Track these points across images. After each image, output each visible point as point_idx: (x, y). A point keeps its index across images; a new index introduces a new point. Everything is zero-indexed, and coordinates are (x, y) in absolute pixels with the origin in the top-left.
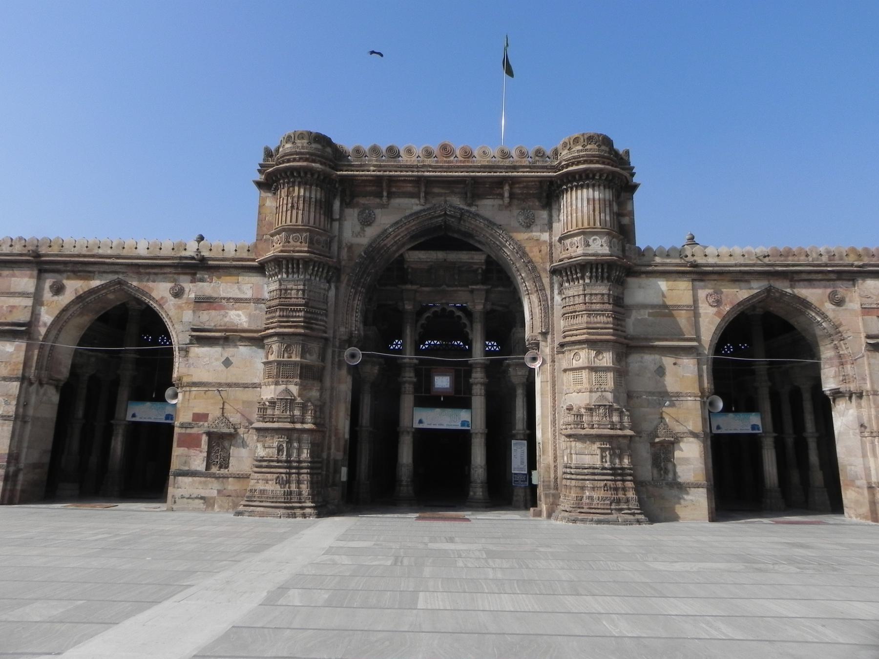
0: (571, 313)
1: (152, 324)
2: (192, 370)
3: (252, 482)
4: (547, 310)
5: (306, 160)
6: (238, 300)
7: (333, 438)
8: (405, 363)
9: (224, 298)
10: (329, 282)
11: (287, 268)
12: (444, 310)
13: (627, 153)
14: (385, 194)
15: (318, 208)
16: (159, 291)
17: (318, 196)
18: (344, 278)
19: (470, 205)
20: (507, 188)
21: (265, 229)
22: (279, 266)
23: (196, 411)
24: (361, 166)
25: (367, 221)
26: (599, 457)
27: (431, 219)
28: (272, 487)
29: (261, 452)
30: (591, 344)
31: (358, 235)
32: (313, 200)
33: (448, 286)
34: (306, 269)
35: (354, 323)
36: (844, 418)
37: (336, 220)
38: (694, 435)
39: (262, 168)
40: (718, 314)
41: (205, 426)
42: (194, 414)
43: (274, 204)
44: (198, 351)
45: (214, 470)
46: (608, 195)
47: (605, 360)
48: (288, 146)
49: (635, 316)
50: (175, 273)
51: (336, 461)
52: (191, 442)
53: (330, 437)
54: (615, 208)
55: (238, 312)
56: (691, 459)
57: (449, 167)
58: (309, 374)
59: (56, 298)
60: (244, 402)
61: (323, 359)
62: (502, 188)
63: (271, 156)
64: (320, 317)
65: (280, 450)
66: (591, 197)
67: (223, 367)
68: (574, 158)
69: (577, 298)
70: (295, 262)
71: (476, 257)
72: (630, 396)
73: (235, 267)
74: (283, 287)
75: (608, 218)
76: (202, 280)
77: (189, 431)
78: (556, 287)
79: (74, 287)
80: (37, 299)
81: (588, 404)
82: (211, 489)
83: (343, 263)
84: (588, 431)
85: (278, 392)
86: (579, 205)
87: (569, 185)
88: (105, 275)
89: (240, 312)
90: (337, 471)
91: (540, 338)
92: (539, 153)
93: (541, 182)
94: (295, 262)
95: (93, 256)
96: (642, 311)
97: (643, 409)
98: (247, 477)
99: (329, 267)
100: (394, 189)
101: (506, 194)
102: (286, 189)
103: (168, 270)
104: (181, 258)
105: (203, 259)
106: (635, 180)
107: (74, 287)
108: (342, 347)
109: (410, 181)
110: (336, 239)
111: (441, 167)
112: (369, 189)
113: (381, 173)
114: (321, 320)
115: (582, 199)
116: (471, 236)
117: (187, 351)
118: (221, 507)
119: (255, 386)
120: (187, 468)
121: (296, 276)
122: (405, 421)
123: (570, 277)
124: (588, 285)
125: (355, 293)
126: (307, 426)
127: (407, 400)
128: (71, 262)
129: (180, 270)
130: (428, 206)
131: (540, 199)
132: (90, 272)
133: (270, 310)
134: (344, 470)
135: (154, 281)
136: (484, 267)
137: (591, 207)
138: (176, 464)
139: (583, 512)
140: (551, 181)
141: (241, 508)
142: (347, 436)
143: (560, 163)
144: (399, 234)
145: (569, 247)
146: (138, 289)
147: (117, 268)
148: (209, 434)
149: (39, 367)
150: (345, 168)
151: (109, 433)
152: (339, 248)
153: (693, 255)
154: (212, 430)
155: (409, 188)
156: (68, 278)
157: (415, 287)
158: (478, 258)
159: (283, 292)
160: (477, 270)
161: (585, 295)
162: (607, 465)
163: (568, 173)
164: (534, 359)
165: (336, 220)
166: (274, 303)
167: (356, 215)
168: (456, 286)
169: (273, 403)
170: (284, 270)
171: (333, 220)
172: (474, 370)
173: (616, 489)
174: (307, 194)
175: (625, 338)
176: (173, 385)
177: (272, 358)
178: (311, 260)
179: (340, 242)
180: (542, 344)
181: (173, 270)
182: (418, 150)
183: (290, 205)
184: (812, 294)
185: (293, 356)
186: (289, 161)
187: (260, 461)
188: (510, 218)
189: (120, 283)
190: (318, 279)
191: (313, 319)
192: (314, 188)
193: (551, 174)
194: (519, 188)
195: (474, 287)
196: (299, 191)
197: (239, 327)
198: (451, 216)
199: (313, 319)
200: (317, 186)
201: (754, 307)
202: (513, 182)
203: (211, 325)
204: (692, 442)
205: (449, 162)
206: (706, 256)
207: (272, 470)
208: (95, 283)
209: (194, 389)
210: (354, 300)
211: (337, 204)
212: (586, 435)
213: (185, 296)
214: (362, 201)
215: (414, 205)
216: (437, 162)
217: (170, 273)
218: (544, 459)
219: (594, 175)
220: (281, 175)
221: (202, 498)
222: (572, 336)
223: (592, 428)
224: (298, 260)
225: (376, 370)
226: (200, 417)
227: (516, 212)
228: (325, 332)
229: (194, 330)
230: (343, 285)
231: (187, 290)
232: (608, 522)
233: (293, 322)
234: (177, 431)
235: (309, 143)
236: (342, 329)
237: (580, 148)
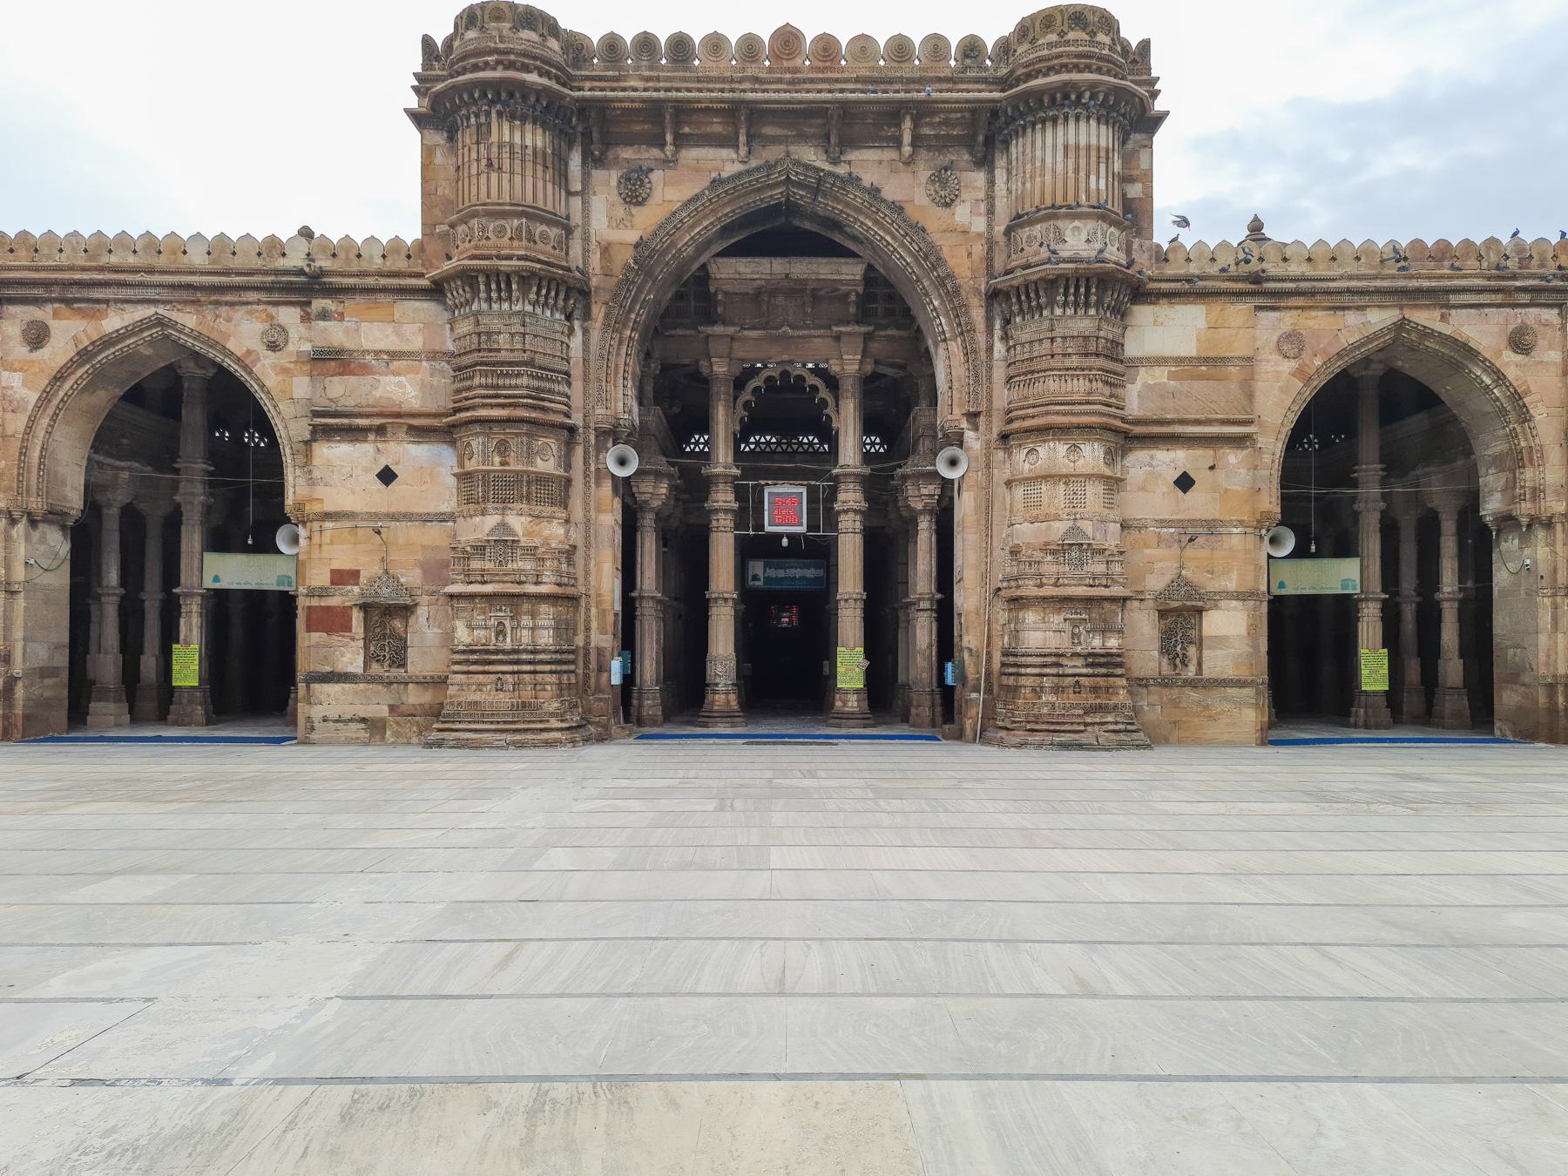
0: (1025, 374)
1: (233, 402)
2: (320, 491)
3: (452, 690)
5: (510, 66)
6: (394, 355)
7: (593, 610)
8: (717, 476)
9: (369, 352)
10: (569, 317)
11: (489, 290)
12: (785, 374)
13: (1145, 46)
14: (669, 138)
15: (540, 168)
16: (240, 335)
17: (539, 144)
18: (598, 312)
19: (835, 162)
20: (907, 124)
21: (437, 212)
22: (471, 286)
23: (336, 565)
24: (617, 79)
26: (1066, 636)
27: (759, 190)
29: (463, 635)
31: (620, 224)
32: (529, 151)
33: (792, 327)
34: (525, 295)
37: (577, 193)
38: (1241, 596)
39: (423, 84)
40: (1299, 372)
42: (333, 571)
43: (452, 161)
44: (332, 453)
45: (376, 668)
47: (1082, 461)
48: (471, 34)
49: (1144, 377)
50: (269, 303)
51: (600, 651)
52: (333, 621)
53: (588, 610)
54: (1117, 166)
55: (398, 379)
56: (1233, 635)
57: (792, 82)
59: (37, 355)
60: (424, 547)
61: (568, 467)
62: (899, 126)
63: (437, 58)
64: (556, 387)
65: (500, 632)
66: (1072, 141)
67: (379, 485)
68: (1041, 60)
69: (1036, 346)
70: (503, 279)
71: (844, 269)
73: (384, 290)
74: (482, 328)
75: (1102, 186)
76: (324, 315)
77: (325, 602)
78: (998, 325)
79: (69, 333)
81: (1047, 544)
83: (594, 282)
84: (1048, 591)
85: (487, 528)
86: (1049, 160)
87: (1030, 118)
88: (128, 307)
89: (402, 379)
90: (603, 668)
91: (964, 424)
92: (972, 47)
93: (973, 111)
94: (503, 279)
95: (101, 269)
96: (1157, 371)
97: (1147, 551)
98: (441, 682)
99: (569, 290)
100: (687, 130)
101: (907, 138)
102: (474, 129)
103: (252, 296)
104: (277, 272)
105: (323, 273)
106: (1159, 105)
107: (69, 333)
108: (600, 448)
109: (718, 112)
110: (578, 233)
111: (780, 81)
112: (637, 128)
113: (662, 94)
114: (559, 394)
115: (1055, 147)
116: (836, 225)
117: (308, 456)
118: (396, 734)
119: (443, 518)
120: (328, 669)
121: (506, 306)
123: (1025, 306)
124: (1060, 318)
125: (620, 343)
126: (543, 589)
128: (55, 283)
129: (276, 297)
130: (753, 163)
131: (971, 147)
132: (98, 301)
134: (616, 666)
135: (229, 320)
136: (860, 289)
137: (1071, 162)
140: (994, 111)
141: (435, 736)
142: (618, 607)
143: (1012, 72)
144: (698, 222)
145: (1025, 246)
146: (198, 337)
147: (150, 294)
148: (364, 607)
149: (21, 488)
150: (588, 84)
152: (586, 251)
153: (1261, 259)
154: (370, 600)
155: (717, 126)
156: (56, 315)
157: (731, 330)
158: (850, 272)
159: (483, 338)
160: (847, 295)
161: (1052, 340)
162: (1079, 649)
163: (1028, 94)
164: (953, 463)
165: (577, 193)
166: (466, 360)
167: (614, 183)
168: (808, 328)
169: (480, 549)
170: (483, 295)
171: (569, 193)
172: (843, 486)
173: (1095, 689)
174: (517, 140)
175: (1123, 420)
176: (288, 521)
177: (471, 465)
178: (533, 274)
179: (586, 239)
180: (969, 435)
181: (263, 296)
183: (484, 162)
184: (1482, 330)
185: (511, 461)
186: (476, 68)
187: (463, 652)
189: (160, 322)
190: (548, 313)
191: (543, 391)
192: (529, 127)
193: (996, 95)
194: (931, 125)
195: (842, 329)
196: (503, 132)
197: (405, 408)
198: (800, 185)
199: (543, 391)
200: (534, 123)
201: (1366, 361)
202: (922, 111)
203: (349, 403)
204: (1235, 609)
205: (796, 70)
206: (1285, 260)
207: (487, 668)
208: (114, 321)
209: (329, 525)
210: (618, 355)
211: (575, 160)
212: (1044, 598)
213: (291, 347)
214: (627, 153)
215: (726, 162)
216: (770, 70)
217: (259, 302)
218: (969, 638)
219: (1079, 96)
220: (461, 98)
221: (363, 720)
222: (1024, 418)
223: (1056, 585)
224: (508, 276)
225: (663, 489)
226: (343, 577)
227: (924, 174)
228: (568, 416)
229: (316, 414)
230: (597, 325)
231: (293, 335)
232: (1080, 746)
233: (506, 397)
234: (302, 602)
235: (515, 29)
236: (600, 411)
237: (1053, 37)
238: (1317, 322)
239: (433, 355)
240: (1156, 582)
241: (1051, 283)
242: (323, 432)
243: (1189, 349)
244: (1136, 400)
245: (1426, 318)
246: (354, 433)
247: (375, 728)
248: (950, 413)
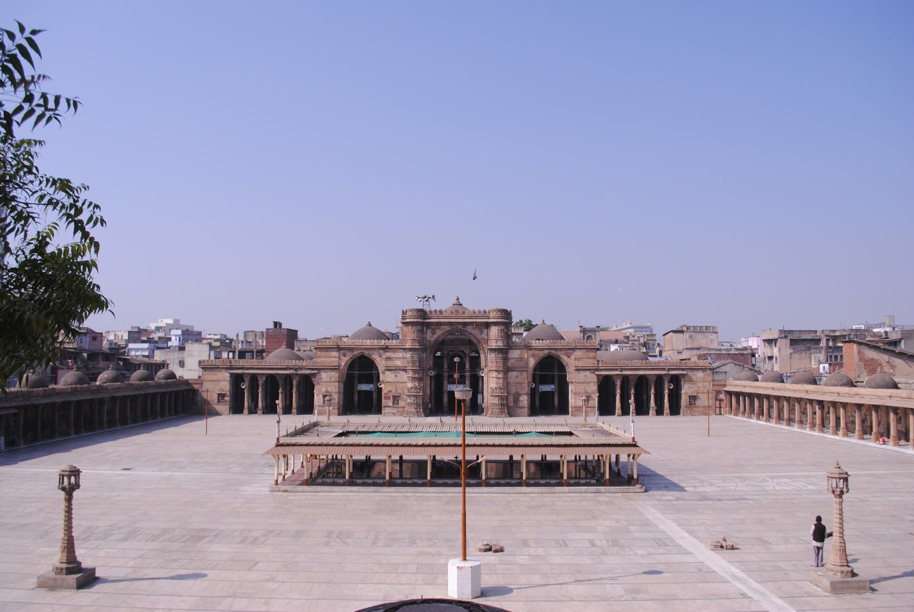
4: (486, 360)
28: (413, 410)
29: (409, 401)
30: (496, 371)
36: (571, 388)
39: (403, 318)
41: (391, 395)
44: (387, 373)
46: (503, 327)
52: (388, 398)
56: (524, 400)
58: (420, 380)
72: (508, 384)
80: (340, 359)
82: (395, 411)
92: (485, 312)
122: (445, 389)
127: (446, 382)
133: (408, 362)
138: (383, 404)
139: (493, 414)
151: (353, 394)
182: (449, 312)
188: (476, 332)
208: (356, 353)
215: (448, 328)
226: (389, 391)
238: (537, 352)
239: (404, 358)
240: (513, 392)
245: (553, 352)
247: (394, 414)
248: (483, 364)
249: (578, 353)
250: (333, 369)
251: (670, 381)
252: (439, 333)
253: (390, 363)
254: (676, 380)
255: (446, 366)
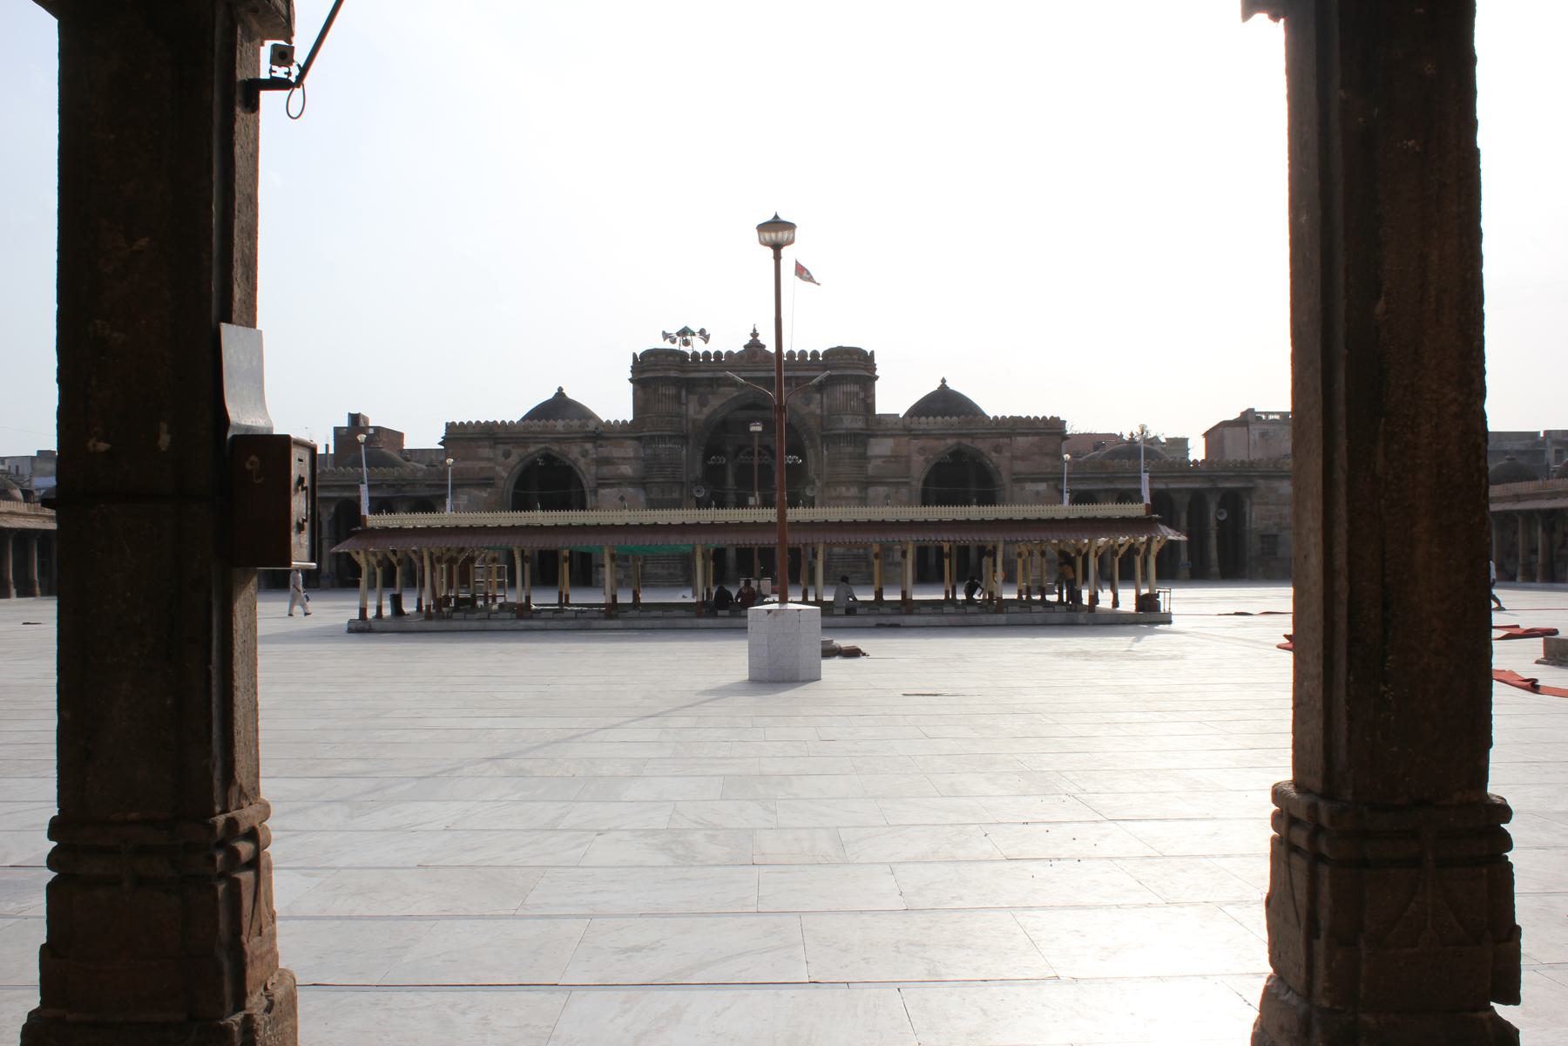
16: (574, 452)
25: (703, 403)
35: (698, 470)
40: (926, 460)
49: (874, 463)
92: (815, 354)
117: (595, 493)
184: (983, 446)
196: (663, 390)
208: (532, 449)
211: (684, 393)
238: (931, 443)
241: (840, 435)
242: (600, 486)
243: (888, 453)
244: (871, 469)
246: (611, 486)
248: (812, 474)
249: (1021, 441)
250: (486, 482)
251: (1222, 505)
252: (715, 403)
253: (606, 471)
254: (1234, 502)
255: (730, 481)
